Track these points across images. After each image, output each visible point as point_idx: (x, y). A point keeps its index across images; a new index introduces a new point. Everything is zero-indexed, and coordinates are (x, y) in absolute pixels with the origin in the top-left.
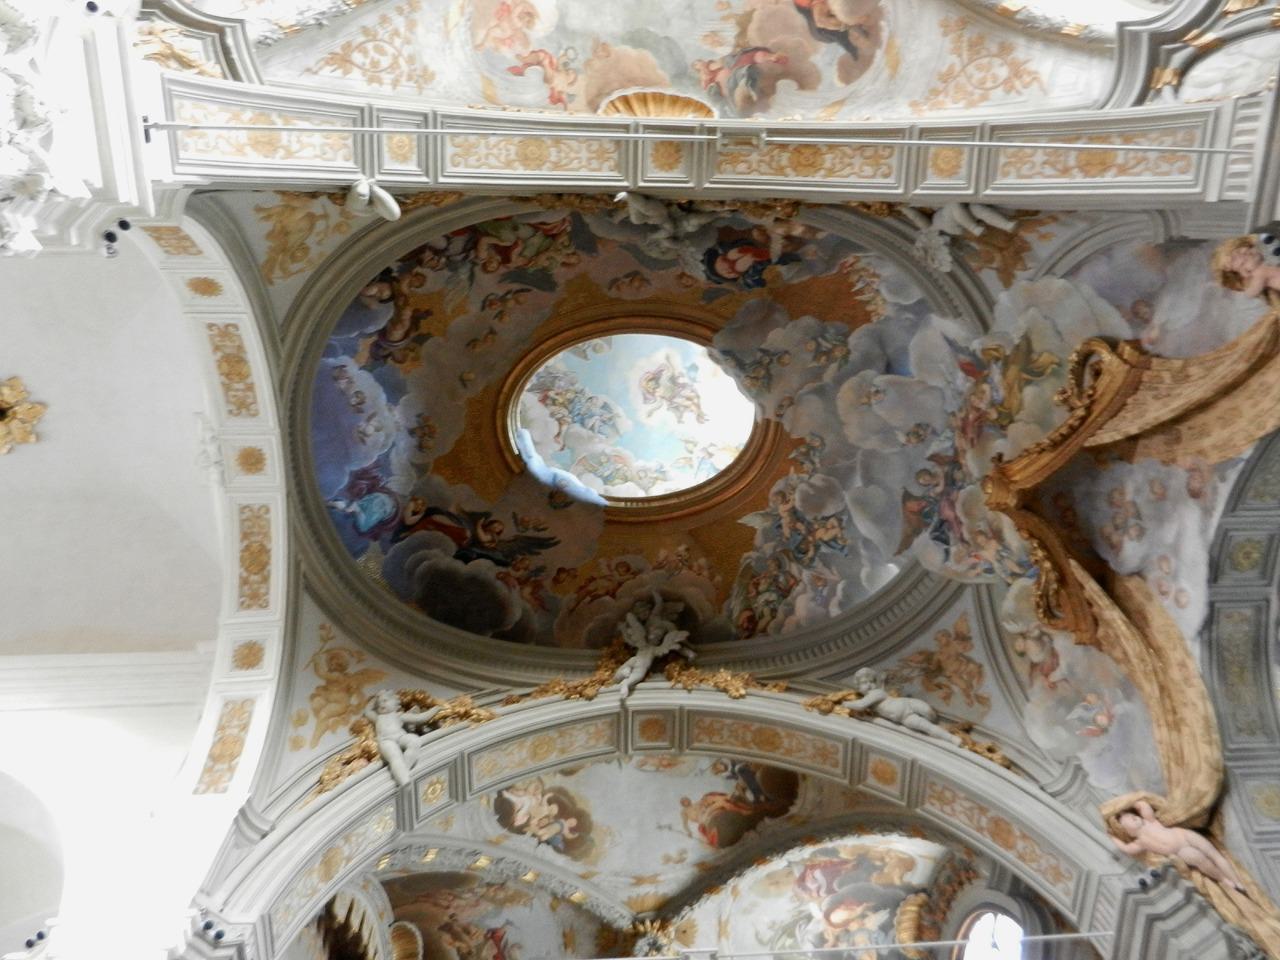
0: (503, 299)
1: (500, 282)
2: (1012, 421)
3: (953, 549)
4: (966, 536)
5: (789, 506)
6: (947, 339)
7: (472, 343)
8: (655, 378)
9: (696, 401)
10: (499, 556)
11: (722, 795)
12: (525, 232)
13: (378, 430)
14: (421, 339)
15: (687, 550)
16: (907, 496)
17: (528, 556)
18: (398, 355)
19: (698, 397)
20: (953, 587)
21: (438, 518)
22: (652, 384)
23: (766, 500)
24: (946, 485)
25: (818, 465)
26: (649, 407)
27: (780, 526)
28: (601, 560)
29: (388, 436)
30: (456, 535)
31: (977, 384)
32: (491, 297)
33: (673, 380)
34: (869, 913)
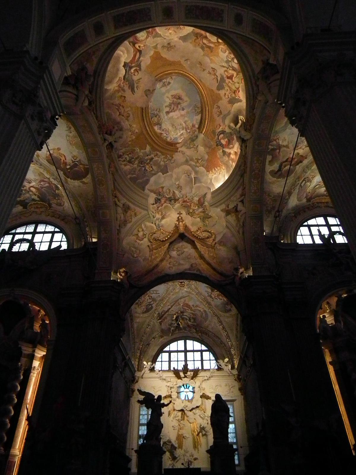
0: (215, 74)
1: (221, 75)
2: (191, 216)
4: (160, 208)
5: (153, 157)
6: (206, 194)
7: (200, 63)
8: (180, 98)
9: (173, 111)
10: (126, 77)
11: (66, 159)
12: (237, 85)
13: (170, 33)
14: (202, 48)
15: (137, 132)
16: (163, 188)
17: (128, 86)
18: (197, 41)
19: (174, 111)
20: (147, 208)
21: (138, 54)
22: (177, 97)
23: (155, 151)
24: (169, 198)
25: (166, 163)
26: (170, 96)
27: (148, 156)
28: (130, 108)
29: (168, 36)
30: (132, 62)
31: (197, 204)
32: (216, 71)
33: (179, 103)
34: (37, 196)
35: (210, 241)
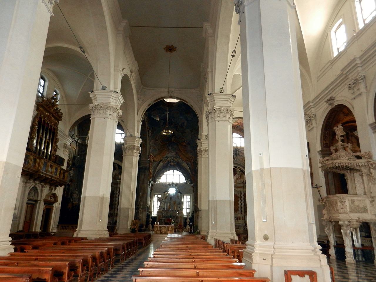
3: (163, 126)
35: (184, 144)
